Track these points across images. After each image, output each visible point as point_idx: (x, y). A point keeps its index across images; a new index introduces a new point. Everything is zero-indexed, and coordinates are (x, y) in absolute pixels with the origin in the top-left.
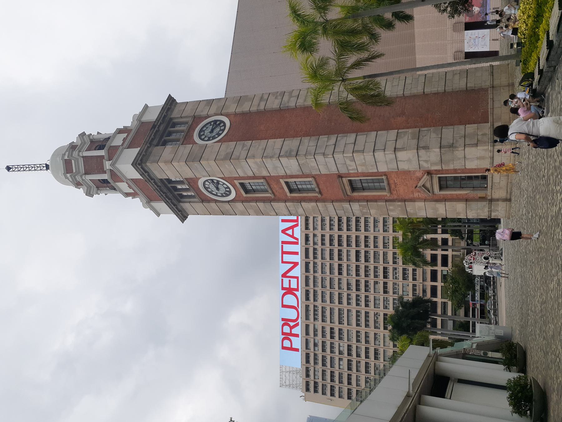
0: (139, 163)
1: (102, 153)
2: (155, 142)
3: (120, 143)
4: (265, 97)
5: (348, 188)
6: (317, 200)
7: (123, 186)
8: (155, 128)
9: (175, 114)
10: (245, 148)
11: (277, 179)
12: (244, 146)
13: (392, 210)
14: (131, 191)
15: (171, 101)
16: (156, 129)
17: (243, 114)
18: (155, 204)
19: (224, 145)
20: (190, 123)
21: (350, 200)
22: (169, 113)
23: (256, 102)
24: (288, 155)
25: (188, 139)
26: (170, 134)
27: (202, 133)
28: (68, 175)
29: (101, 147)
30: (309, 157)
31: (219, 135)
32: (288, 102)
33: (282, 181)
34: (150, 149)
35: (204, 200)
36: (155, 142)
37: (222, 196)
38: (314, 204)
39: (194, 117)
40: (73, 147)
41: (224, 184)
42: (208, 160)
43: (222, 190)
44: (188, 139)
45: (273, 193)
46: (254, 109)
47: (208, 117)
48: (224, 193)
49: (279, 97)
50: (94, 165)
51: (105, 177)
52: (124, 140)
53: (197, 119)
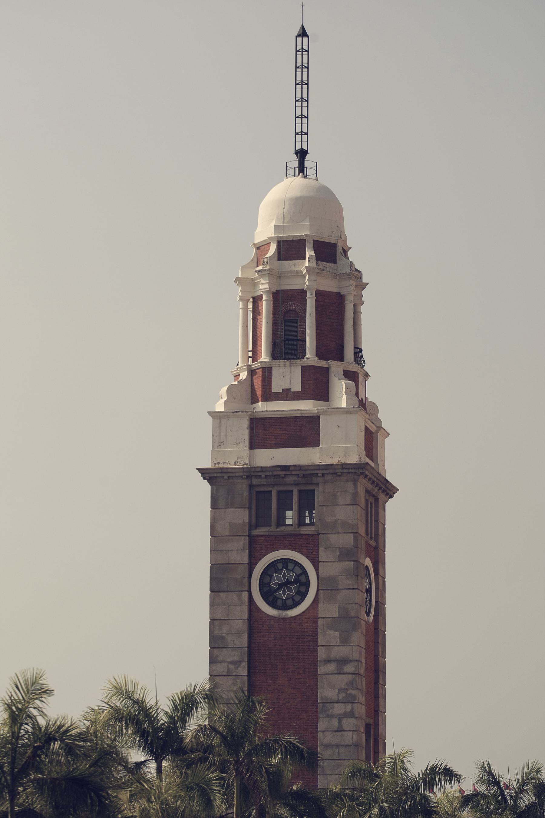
2: (255, 481)
3: (276, 388)
8: (282, 470)
10: (232, 667)
12: (236, 663)
16: (282, 473)
27: (280, 566)
31: (272, 604)
32: (328, 716)
42: (212, 605)
46: (322, 654)
49: (342, 695)
53: (310, 545)
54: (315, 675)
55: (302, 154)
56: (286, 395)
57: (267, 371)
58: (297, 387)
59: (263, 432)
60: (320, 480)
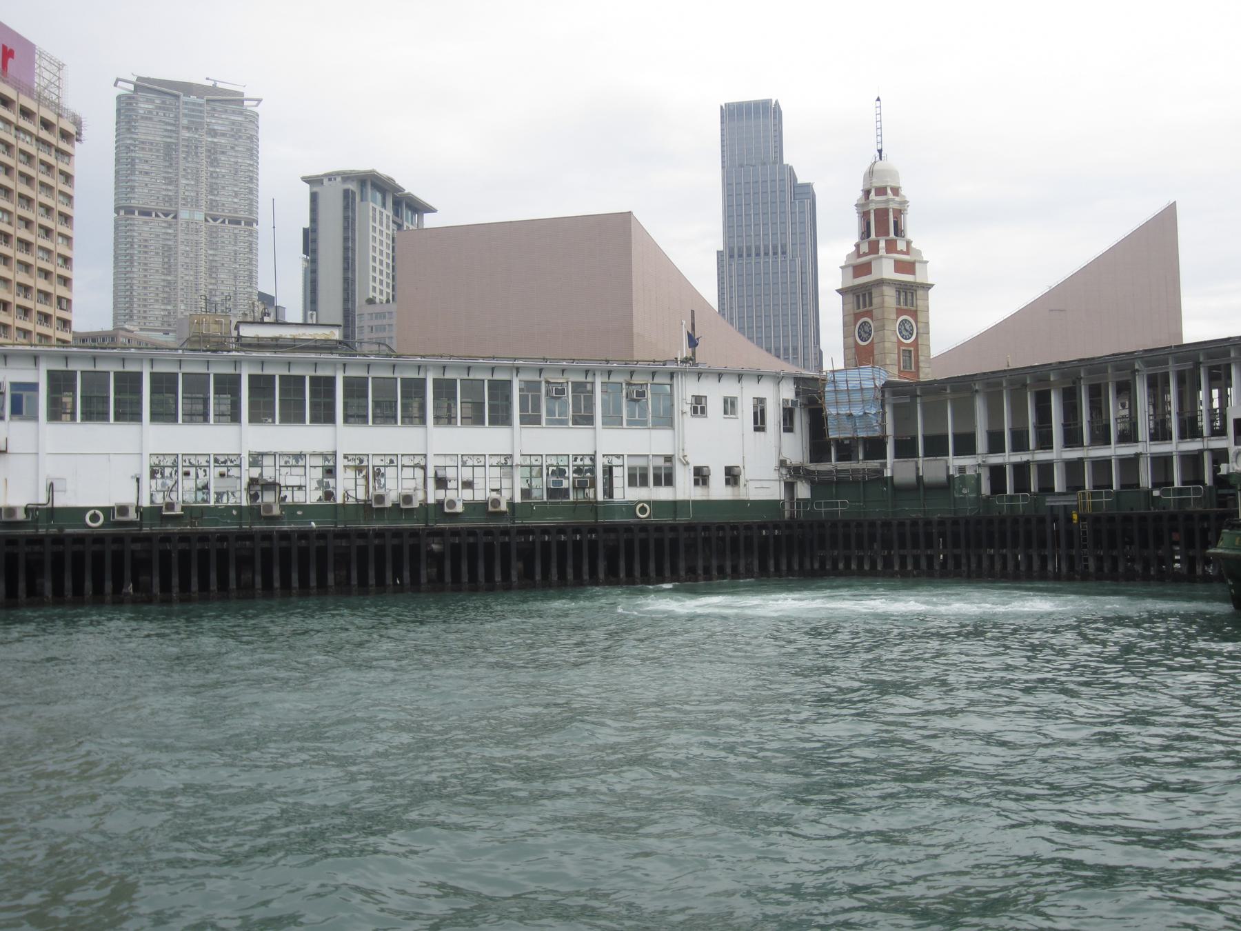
1: (892, 235)
7: (865, 248)
15: (928, 287)
18: (850, 270)
28: (873, 192)
29: (896, 234)
35: (857, 317)
39: (916, 311)
40: (896, 191)
43: (864, 335)
47: (916, 322)
51: (873, 236)
52: (901, 252)
55: (880, 151)
56: (901, 252)
57: (895, 241)
59: (901, 267)
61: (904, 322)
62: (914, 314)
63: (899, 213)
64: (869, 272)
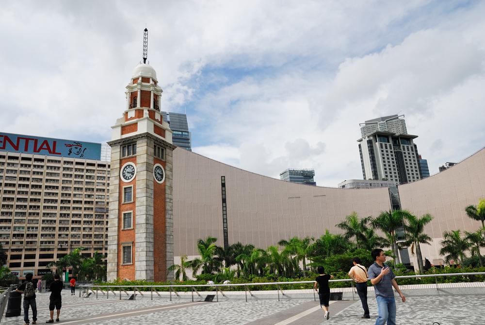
0: (147, 136)
4: (171, 201)
5: (126, 245)
6: (119, 227)
7: (132, 114)
9: (168, 150)
11: (133, 208)
12: (151, 194)
13: (112, 265)
14: (129, 117)
17: (165, 190)
18: (119, 129)
19: (152, 183)
20: (163, 160)
21: (118, 245)
22: (169, 147)
23: (170, 196)
24: (147, 219)
25: (156, 161)
26: (159, 148)
28: (140, 79)
30: (145, 230)
31: (156, 178)
33: (132, 211)
34: (153, 140)
36: (156, 142)
37: (123, 173)
38: (117, 225)
39: (165, 162)
40: (155, 82)
41: (131, 178)
42: (147, 175)
43: (128, 175)
44: (156, 161)
45: (123, 204)
46: (167, 196)
47: (165, 170)
48: (125, 175)
50: (145, 95)
52: (157, 120)
54: (165, 202)
55: (145, 59)
58: (160, 120)
60: (167, 147)
61: (158, 168)
62: (164, 164)
63: (156, 97)
64: (135, 130)
